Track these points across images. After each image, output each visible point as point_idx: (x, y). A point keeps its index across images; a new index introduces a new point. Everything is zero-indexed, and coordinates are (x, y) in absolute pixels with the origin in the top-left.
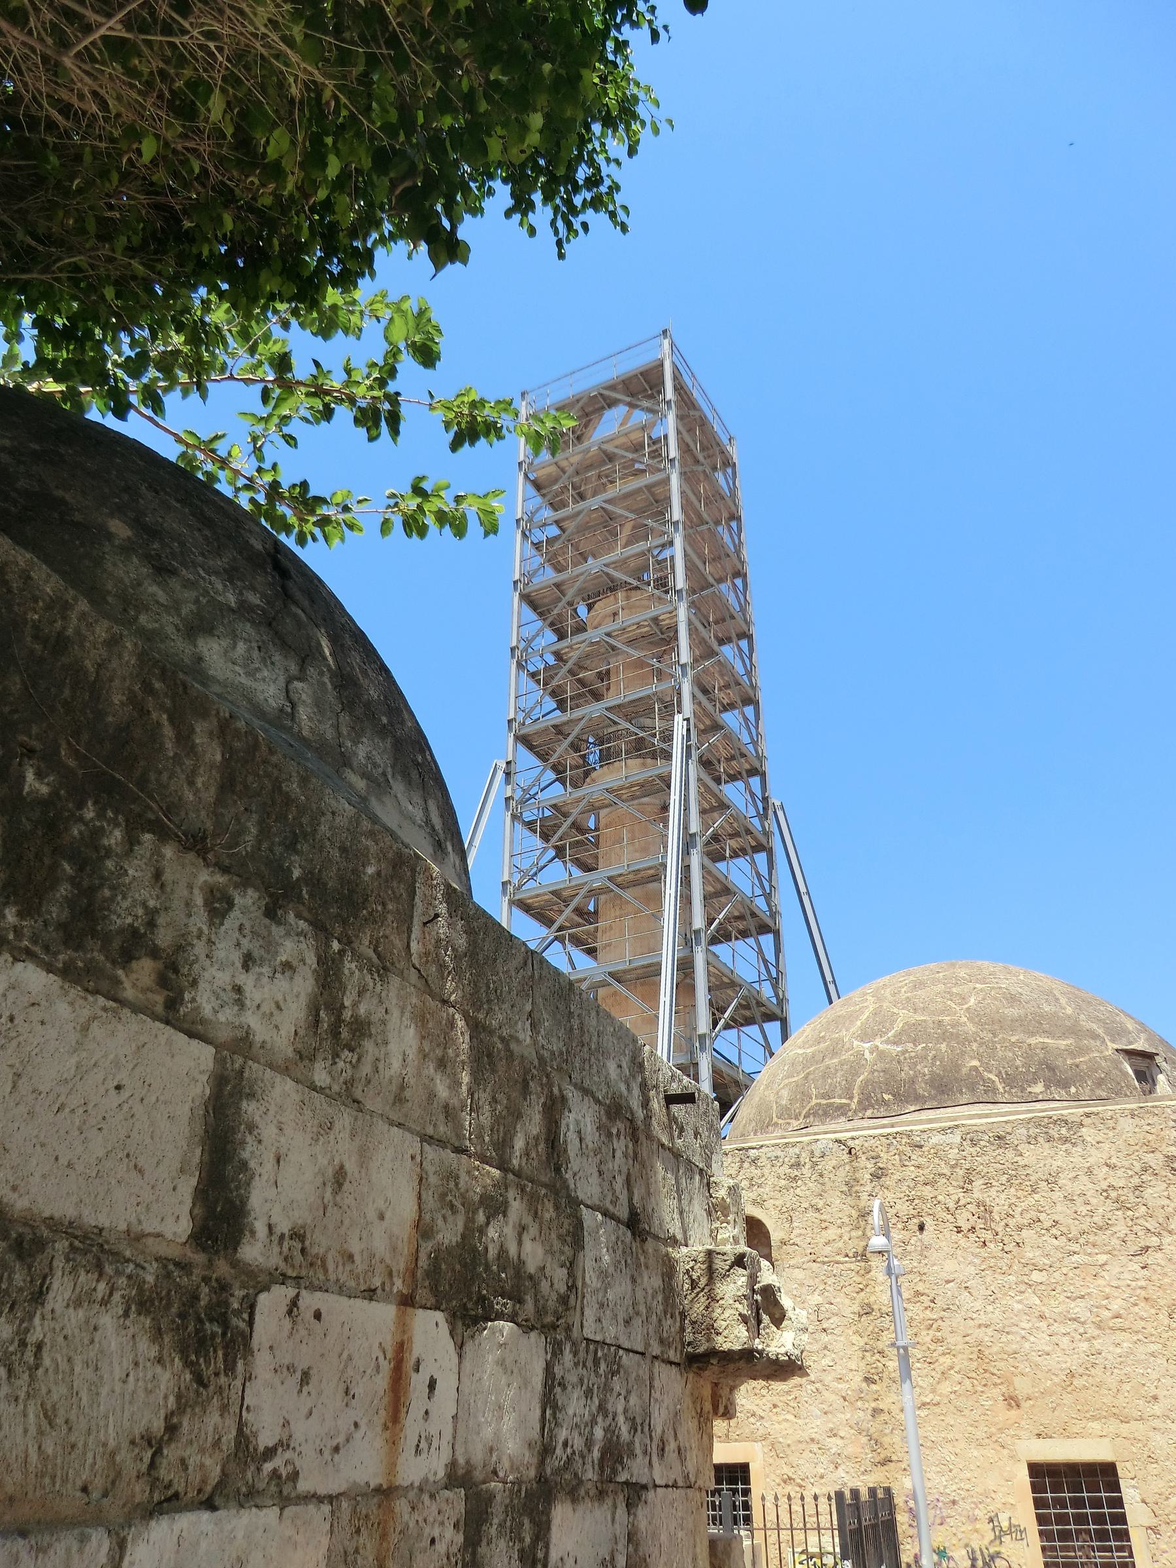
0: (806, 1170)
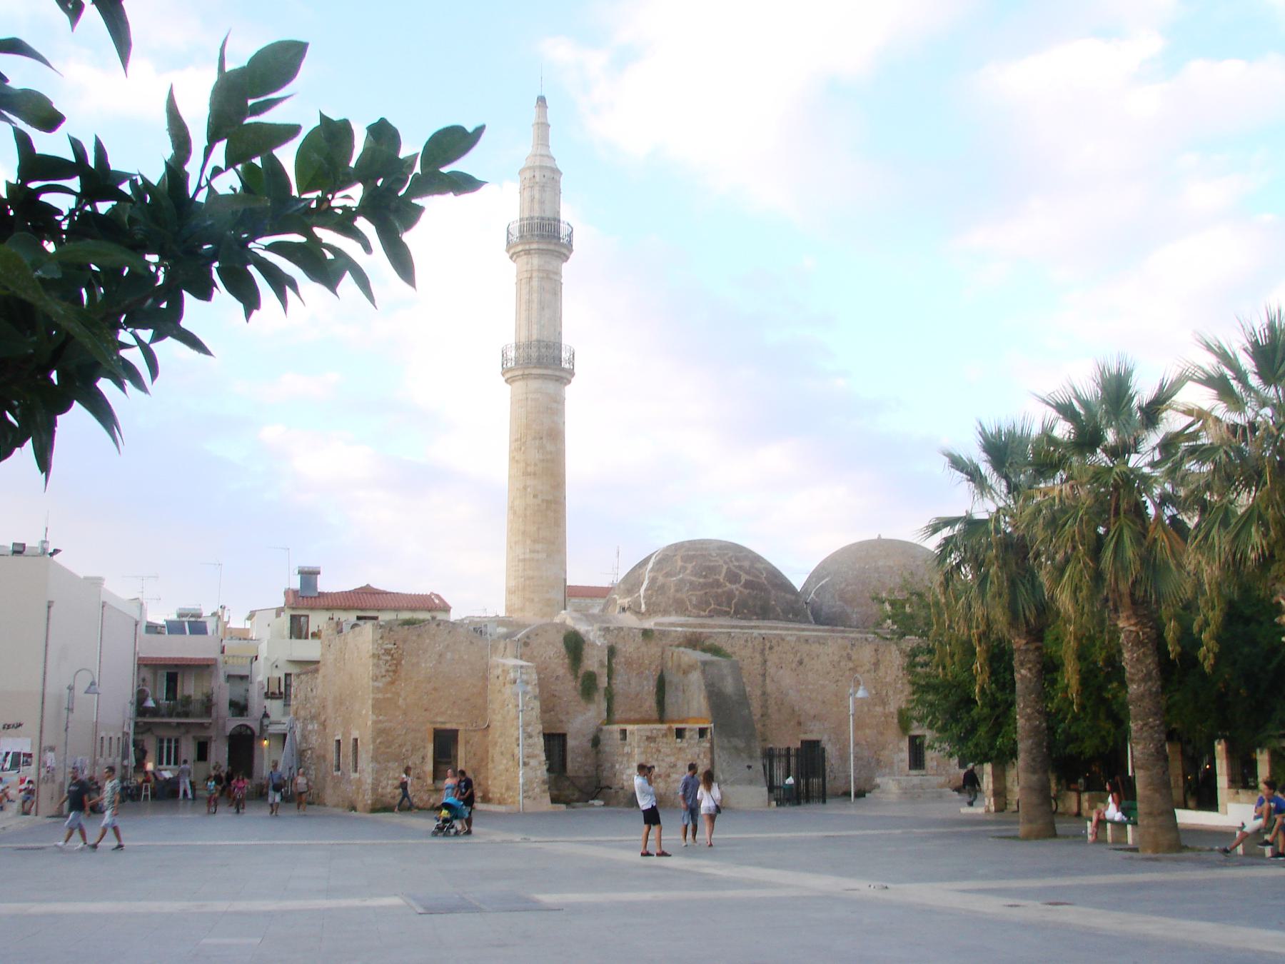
0: (750, 643)
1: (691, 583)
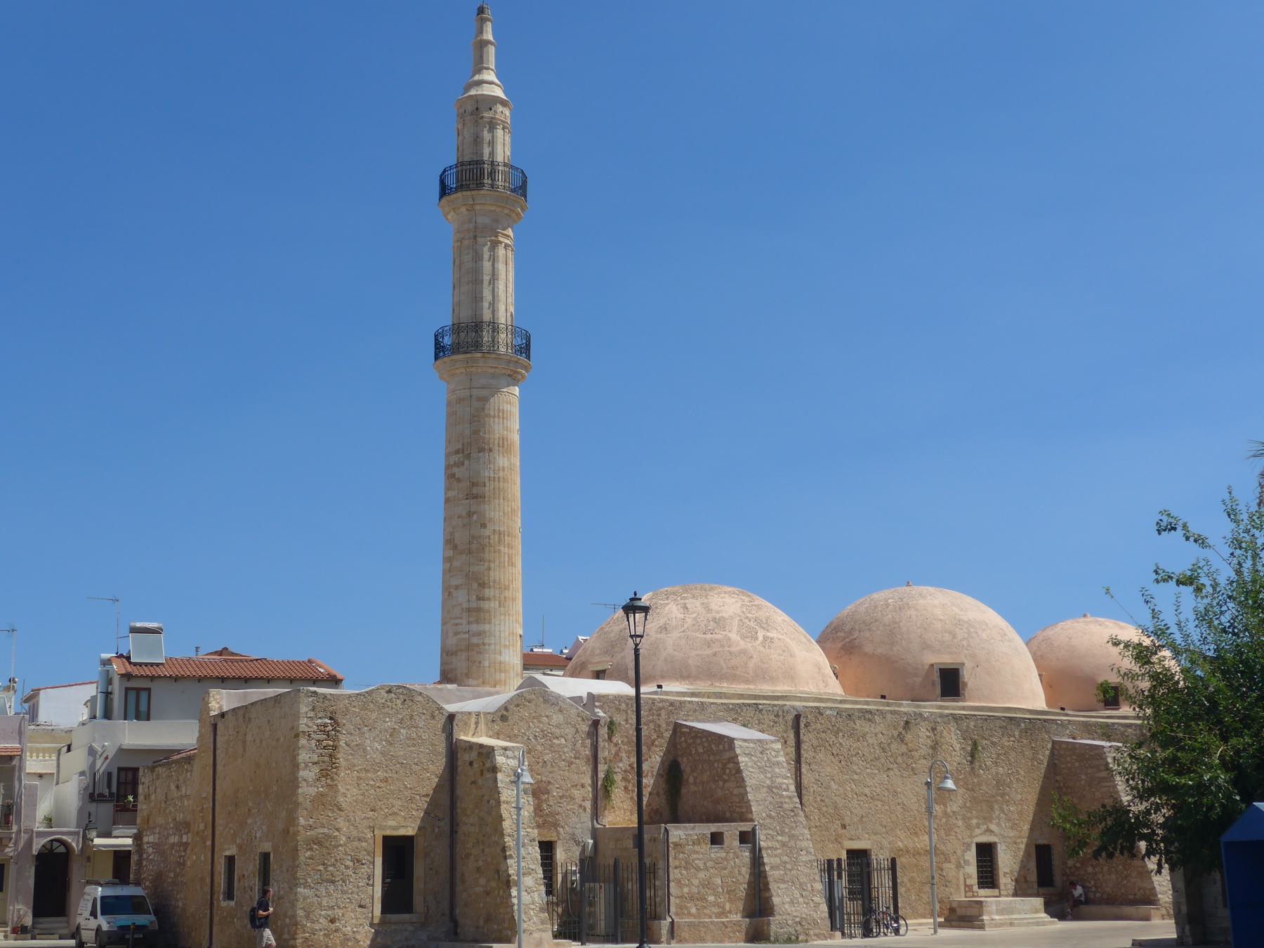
0: (781, 719)
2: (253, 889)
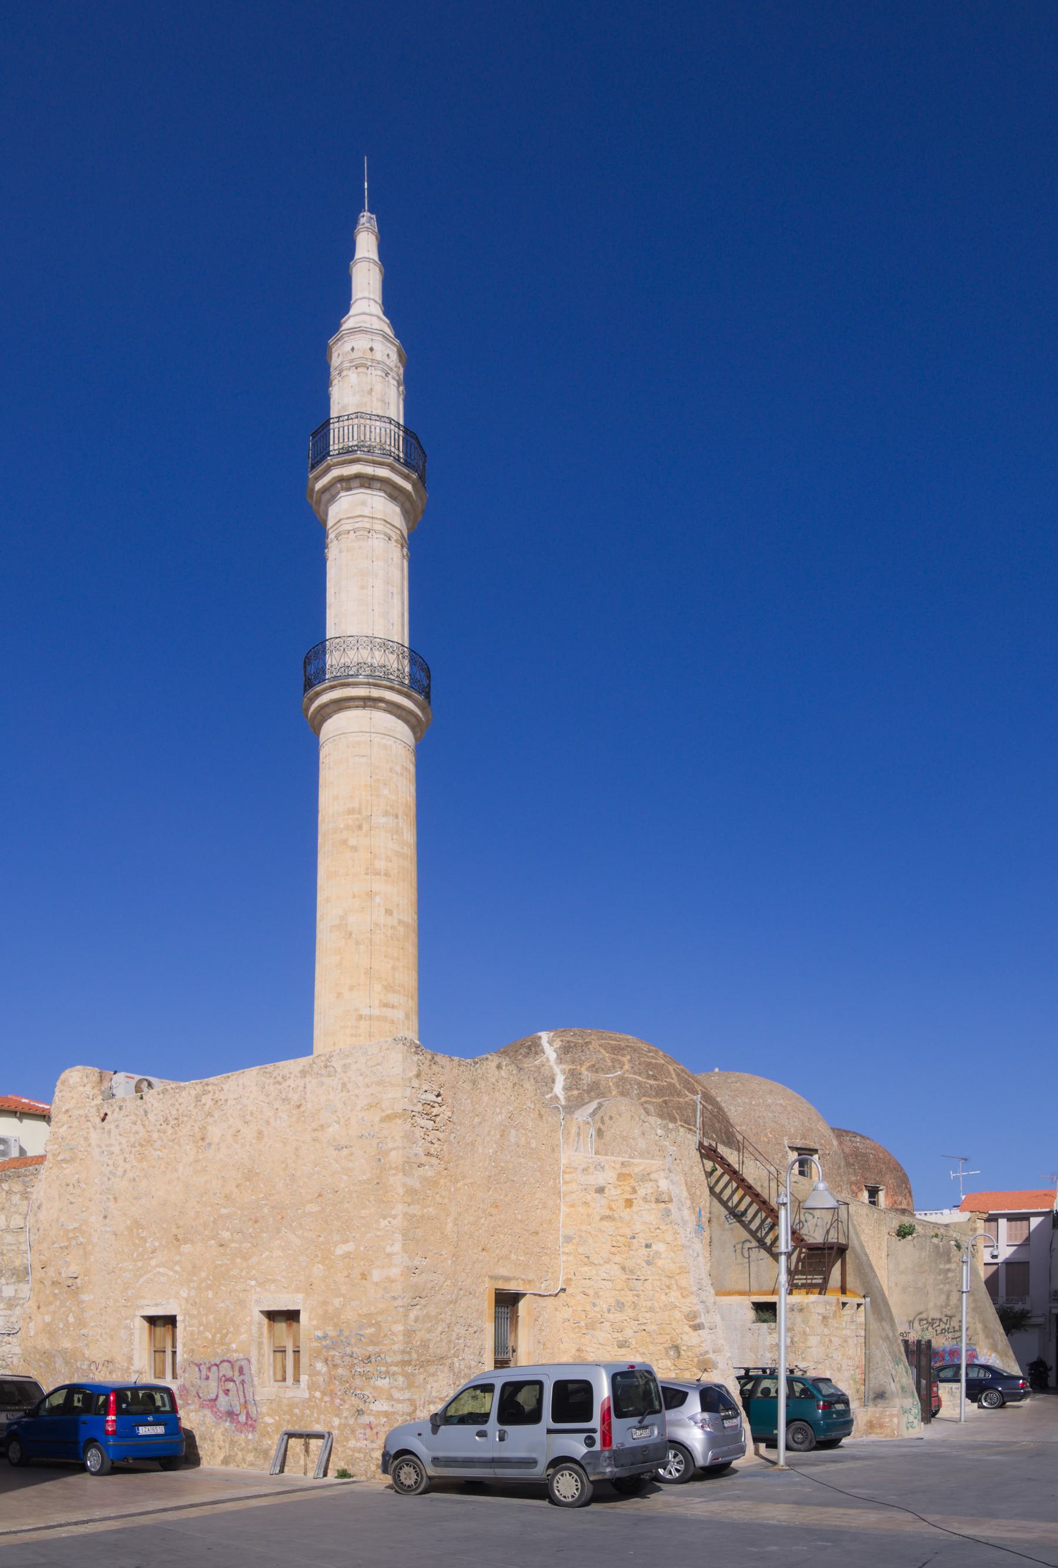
1: (640, 1084)
2: (245, 1370)
